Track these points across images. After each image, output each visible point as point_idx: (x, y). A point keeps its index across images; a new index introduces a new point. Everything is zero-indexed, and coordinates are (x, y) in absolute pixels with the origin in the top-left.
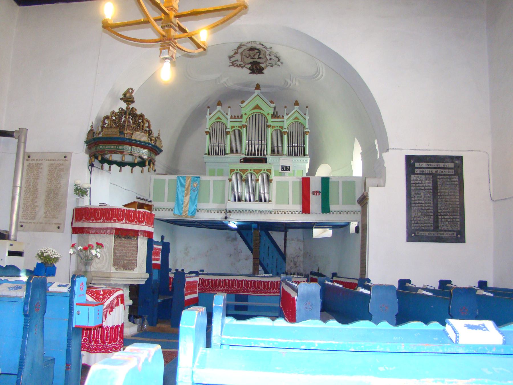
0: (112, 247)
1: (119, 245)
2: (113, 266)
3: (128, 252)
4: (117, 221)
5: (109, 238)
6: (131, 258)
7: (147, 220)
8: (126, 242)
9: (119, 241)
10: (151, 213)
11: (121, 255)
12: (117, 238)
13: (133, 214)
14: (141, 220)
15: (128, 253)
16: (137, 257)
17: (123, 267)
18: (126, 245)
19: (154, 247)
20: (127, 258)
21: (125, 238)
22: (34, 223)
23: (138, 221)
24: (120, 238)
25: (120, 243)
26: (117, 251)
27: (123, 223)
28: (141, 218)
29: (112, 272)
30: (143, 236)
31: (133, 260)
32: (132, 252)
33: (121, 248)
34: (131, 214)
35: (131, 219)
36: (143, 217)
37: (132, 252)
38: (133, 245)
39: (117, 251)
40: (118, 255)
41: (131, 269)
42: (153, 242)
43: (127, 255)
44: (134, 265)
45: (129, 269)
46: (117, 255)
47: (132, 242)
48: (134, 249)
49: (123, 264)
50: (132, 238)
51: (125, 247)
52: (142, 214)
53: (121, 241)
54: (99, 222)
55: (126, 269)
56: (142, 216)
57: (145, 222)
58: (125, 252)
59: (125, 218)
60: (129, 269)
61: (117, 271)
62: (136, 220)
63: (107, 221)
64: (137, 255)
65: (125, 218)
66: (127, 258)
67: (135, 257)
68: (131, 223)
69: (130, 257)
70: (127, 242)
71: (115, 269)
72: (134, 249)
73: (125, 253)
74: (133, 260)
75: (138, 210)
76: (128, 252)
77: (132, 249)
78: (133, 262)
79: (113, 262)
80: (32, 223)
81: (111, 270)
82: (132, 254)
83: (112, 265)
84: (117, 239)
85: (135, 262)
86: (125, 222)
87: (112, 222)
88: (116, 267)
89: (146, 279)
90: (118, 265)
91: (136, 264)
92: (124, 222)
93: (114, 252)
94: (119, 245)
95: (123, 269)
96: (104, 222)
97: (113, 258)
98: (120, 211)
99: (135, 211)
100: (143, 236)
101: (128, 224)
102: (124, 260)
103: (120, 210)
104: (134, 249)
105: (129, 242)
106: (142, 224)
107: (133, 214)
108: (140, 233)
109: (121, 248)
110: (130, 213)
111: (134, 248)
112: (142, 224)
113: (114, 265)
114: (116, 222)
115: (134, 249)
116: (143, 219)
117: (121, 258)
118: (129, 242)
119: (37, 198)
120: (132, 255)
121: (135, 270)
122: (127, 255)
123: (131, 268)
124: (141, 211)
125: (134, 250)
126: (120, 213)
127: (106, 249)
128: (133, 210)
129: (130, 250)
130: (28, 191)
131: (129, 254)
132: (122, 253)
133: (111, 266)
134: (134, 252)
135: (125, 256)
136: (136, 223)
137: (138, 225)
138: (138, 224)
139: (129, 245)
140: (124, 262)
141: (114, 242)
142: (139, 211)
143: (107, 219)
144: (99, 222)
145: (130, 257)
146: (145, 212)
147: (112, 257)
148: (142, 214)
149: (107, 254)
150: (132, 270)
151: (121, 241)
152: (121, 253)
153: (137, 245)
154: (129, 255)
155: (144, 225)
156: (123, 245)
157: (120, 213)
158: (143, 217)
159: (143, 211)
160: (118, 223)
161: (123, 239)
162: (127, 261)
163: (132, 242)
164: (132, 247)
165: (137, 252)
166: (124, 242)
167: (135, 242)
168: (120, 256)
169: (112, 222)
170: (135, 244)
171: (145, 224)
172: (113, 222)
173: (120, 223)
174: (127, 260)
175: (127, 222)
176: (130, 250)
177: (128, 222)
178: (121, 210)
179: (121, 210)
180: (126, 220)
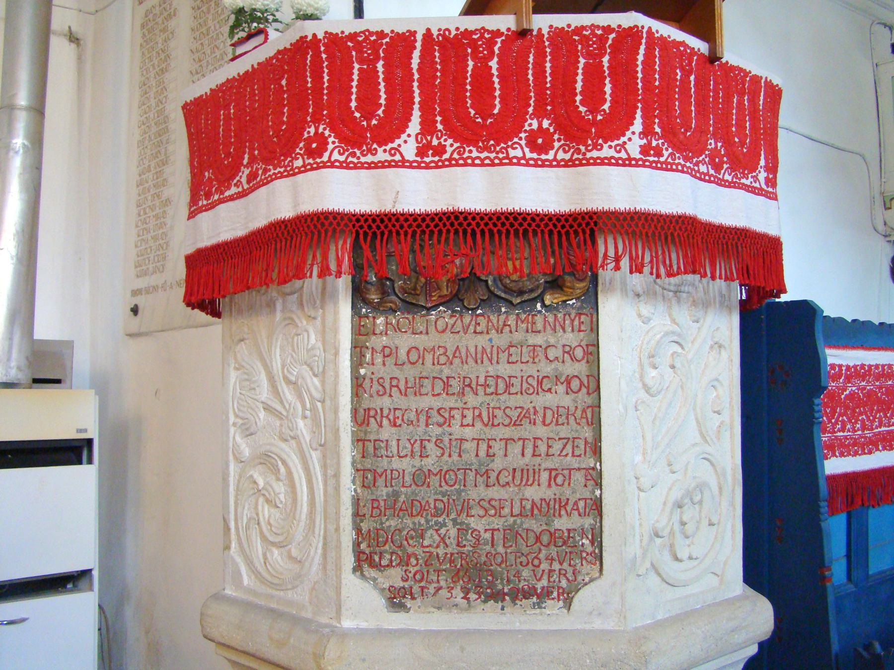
0: (335, 397)
1: (410, 372)
2: (357, 569)
3: (507, 432)
4: (334, 151)
5: (318, 322)
6: (533, 493)
7: (667, 110)
8: (471, 342)
9: (404, 342)
10: (713, 58)
11: (429, 463)
12: (377, 308)
13: (494, 64)
14: (594, 109)
15: (497, 447)
16: (596, 478)
17: (456, 576)
18: (478, 372)
19: (830, 361)
20: (495, 493)
21: (454, 300)
22: (164, 287)
23: (560, 127)
24: (411, 307)
25: (417, 355)
26: (387, 432)
27: (403, 164)
28: (593, 97)
29: (347, 623)
30: (625, 263)
31: (561, 506)
32: (541, 431)
33: (426, 402)
34: (482, 73)
35: (485, 112)
36: (608, 89)
37: (541, 431)
38: (548, 369)
39: (387, 432)
40: (407, 465)
41: (546, 594)
42: (818, 327)
43: (498, 464)
44: (576, 551)
45: (527, 595)
46: (396, 464)
47: (539, 340)
48: (559, 398)
49: (453, 548)
50: (534, 300)
51: (468, 385)
52: (595, 56)
53: (421, 341)
54: (233, 190)
55: (497, 596)
56: (594, 75)
57: (638, 125)
58: (468, 433)
59: (416, 115)
60: (519, 594)
61: (398, 620)
62: (539, 114)
63: (265, 171)
64: (596, 450)
65: (416, 115)
66: (495, 493)
67: (578, 477)
68: (486, 148)
69: (527, 476)
70: (482, 341)
71: (380, 602)
72: (559, 398)
73: (469, 446)
74: (561, 506)
75: (543, 23)
76: (507, 432)
77: (548, 399)
78: (562, 523)
79: (359, 531)
80: (160, 290)
81: (339, 616)
82: (543, 448)
83: (348, 560)
84: (380, 320)
85: (588, 522)
86: (421, 152)
87: (299, 163)
88: (394, 577)
89: (753, 650)
90: (405, 562)
91: (597, 538)
92: (409, 150)
93: (359, 441)
94: (410, 372)
95: (466, 592)
96: (256, 183)
97: (356, 502)
98: (360, 52)
99: (523, 33)
100: (625, 263)
101: (451, 163)
102: (466, 508)
103: (358, 46)
104: (567, 401)
105: (501, 341)
106: (606, 152)
107: (494, 64)
108: (606, 246)
109: (426, 402)
110: (471, 63)
111: (561, 389)
112: (606, 152)
113: (372, 565)
114: (325, 158)
115: (567, 401)
116: (606, 107)
117: (427, 495)
118: (501, 341)
119: (164, 163)
120: (549, 464)
121: (583, 598)
122: (498, 464)
123: (539, 586)
124: (579, 30)
125: (559, 416)
126: (369, 78)
127: (304, 417)
128: (497, 33)
129: (526, 416)
130: (147, 142)
131: (515, 448)
132: (438, 442)
133: (338, 568)
134: (564, 431)
135: (471, 475)
136: (544, 148)
137: (567, 164)
138: (561, 155)
139: (504, 369)
140: (463, 530)
141: (358, 350)
142: (558, 34)
143: (270, 158)
144: (233, 190)
145: (527, 476)
146: (632, 35)
147: (348, 488)
148: (595, 56)
149: (315, 457)
150: (553, 606)
151: (421, 341)
152: (430, 446)
153: (592, 352)
154: (516, 458)
155: (629, 162)
156: (446, 371)
157: (369, 78)
158: (608, 89)
159: (608, 29)
160: (345, 166)
161: (443, 317)
162: (498, 523)
163: (539, 340)
164: (540, 385)
165: (596, 423)
166: (450, 341)
167: (571, 338)
168: (421, 478)
169: (299, 163)
170: (569, 352)
171: (635, 153)
172: (304, 169)
173: (371, 166)
174: (493, 507)
175: (440, 150)
176: (526, 416)
177: (450, 145)
178: (375, 46)
179: (375, 46)
180: (427, 127)
